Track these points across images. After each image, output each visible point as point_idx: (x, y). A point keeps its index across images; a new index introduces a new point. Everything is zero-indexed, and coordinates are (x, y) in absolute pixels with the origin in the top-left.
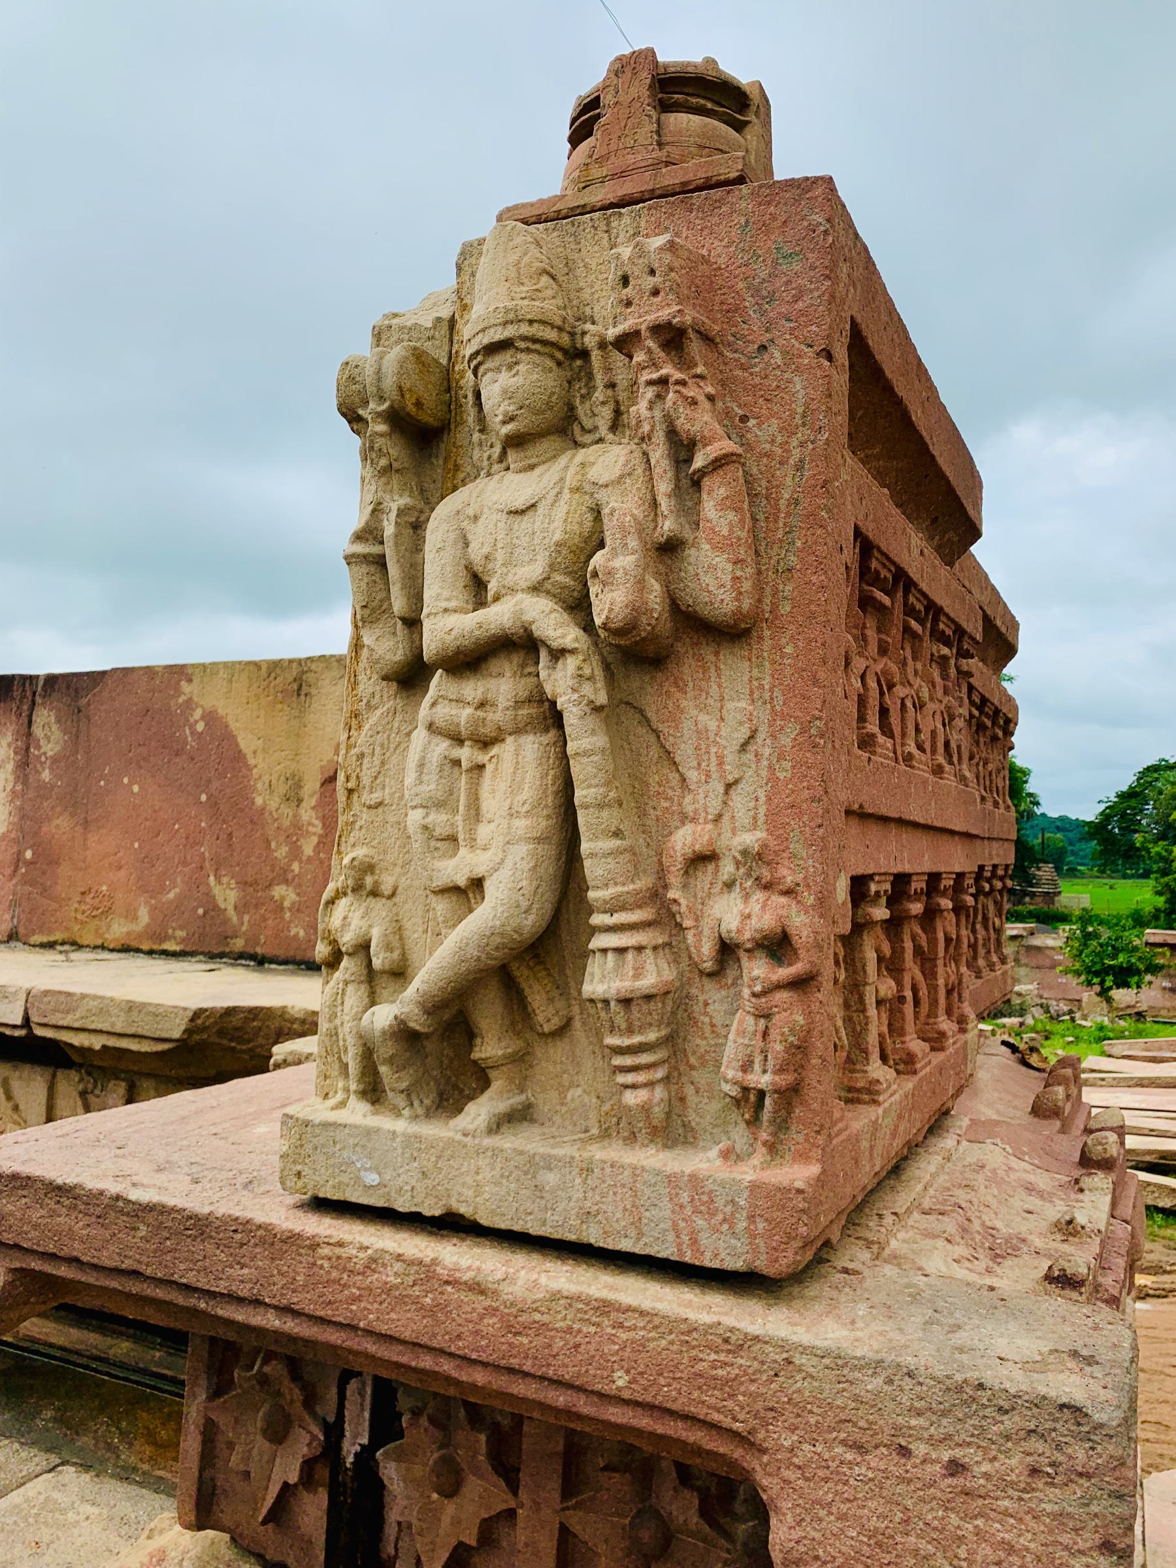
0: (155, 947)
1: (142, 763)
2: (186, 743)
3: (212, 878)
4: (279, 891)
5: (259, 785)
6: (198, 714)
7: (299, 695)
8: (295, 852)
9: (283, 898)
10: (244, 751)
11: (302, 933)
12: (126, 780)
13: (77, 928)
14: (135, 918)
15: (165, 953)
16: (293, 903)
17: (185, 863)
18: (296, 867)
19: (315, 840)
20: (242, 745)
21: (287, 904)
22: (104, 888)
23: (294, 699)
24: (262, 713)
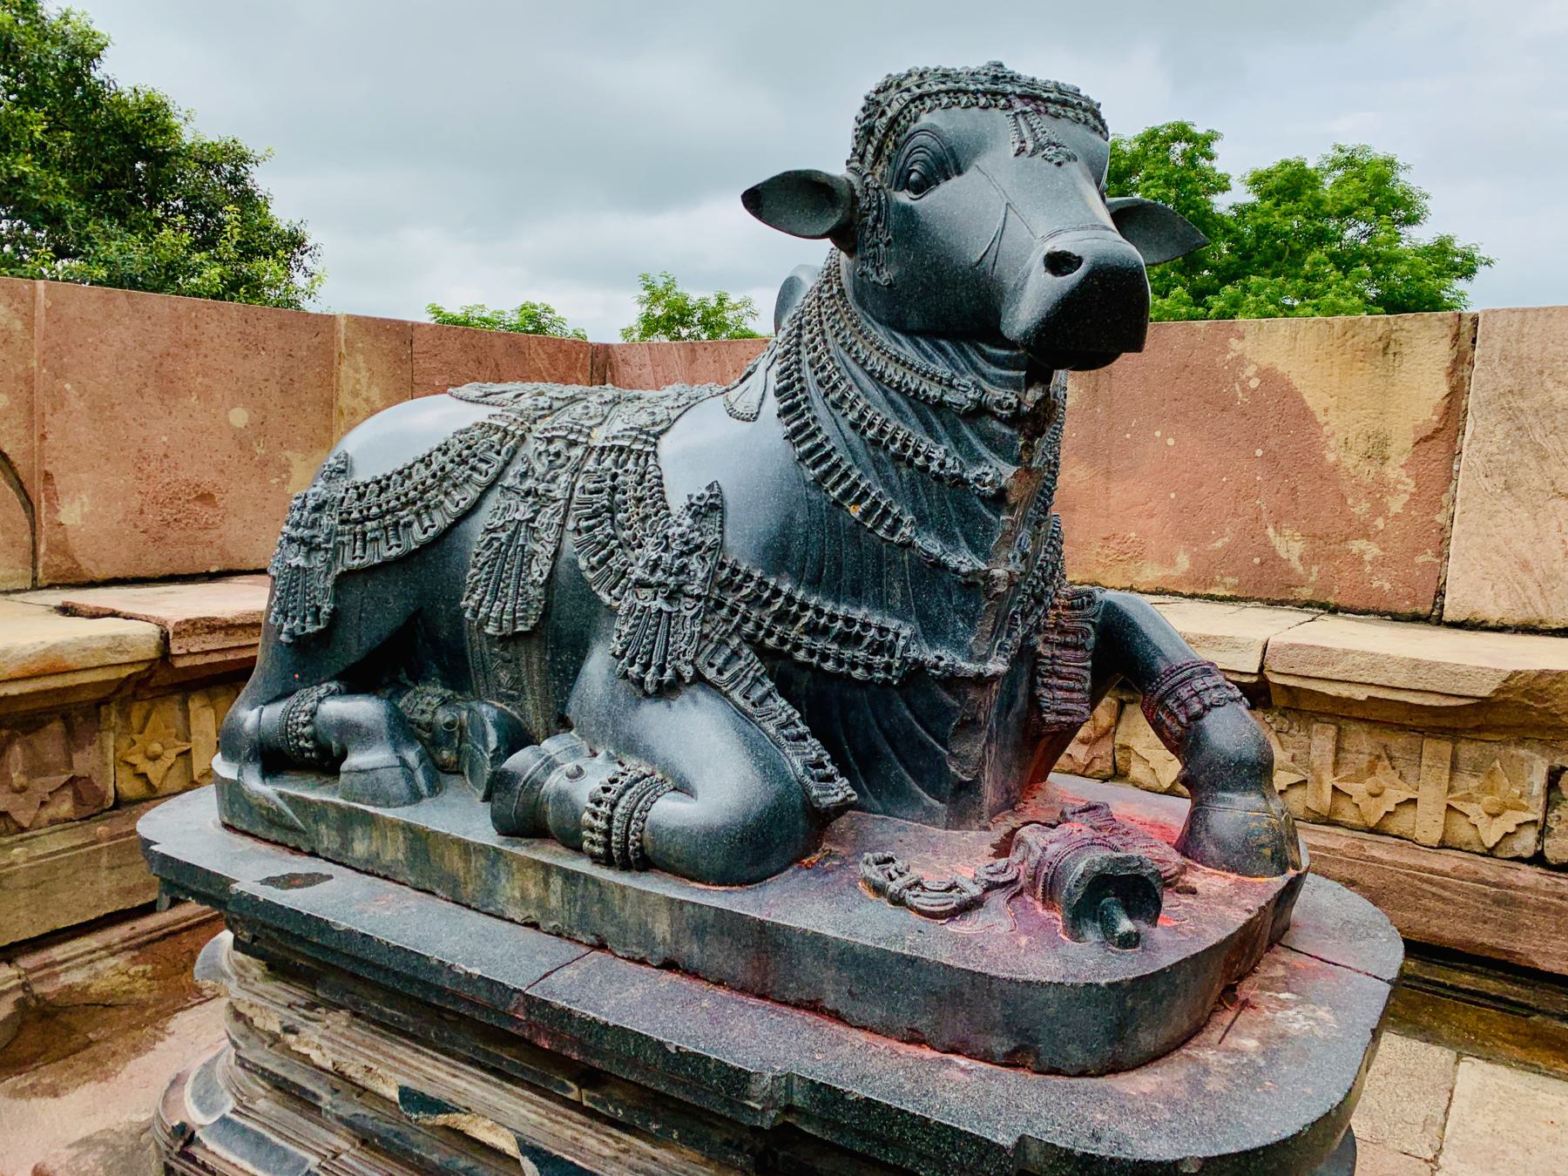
0: (1198, 592)
2: (1235, 398)
3: (1271, 530)
4: (1357, 546)
5: (1332, 443)
6: (1251, 370)
7: (1385, 354)
8: (1379, 509)
9: (1362, 553)
11: (1387, 586)
12: (1158, 434)
13: (1099, 570)
14: (1173, 564)
15: (1212, 598)
16: (1375, 558)
17: (1235, 514)
18: (1380, 523)
19: (1406, 497)
20: (1310, 402)
21: (1367, 558)
23: (1380, 358)
24: (1336, 371)
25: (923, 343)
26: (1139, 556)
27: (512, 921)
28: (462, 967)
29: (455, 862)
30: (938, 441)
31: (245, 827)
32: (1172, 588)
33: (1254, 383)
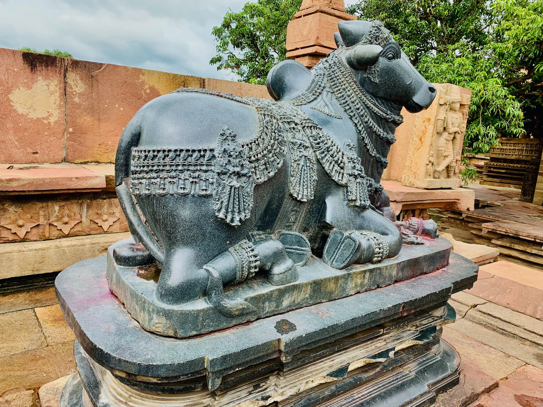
1: (124, 100)
12: (117, 106)
22: (110, 143)
25: (379, 101)
27: (351, 295)
28: (386, 308)
29: (332, 286)
33: (148, 91)
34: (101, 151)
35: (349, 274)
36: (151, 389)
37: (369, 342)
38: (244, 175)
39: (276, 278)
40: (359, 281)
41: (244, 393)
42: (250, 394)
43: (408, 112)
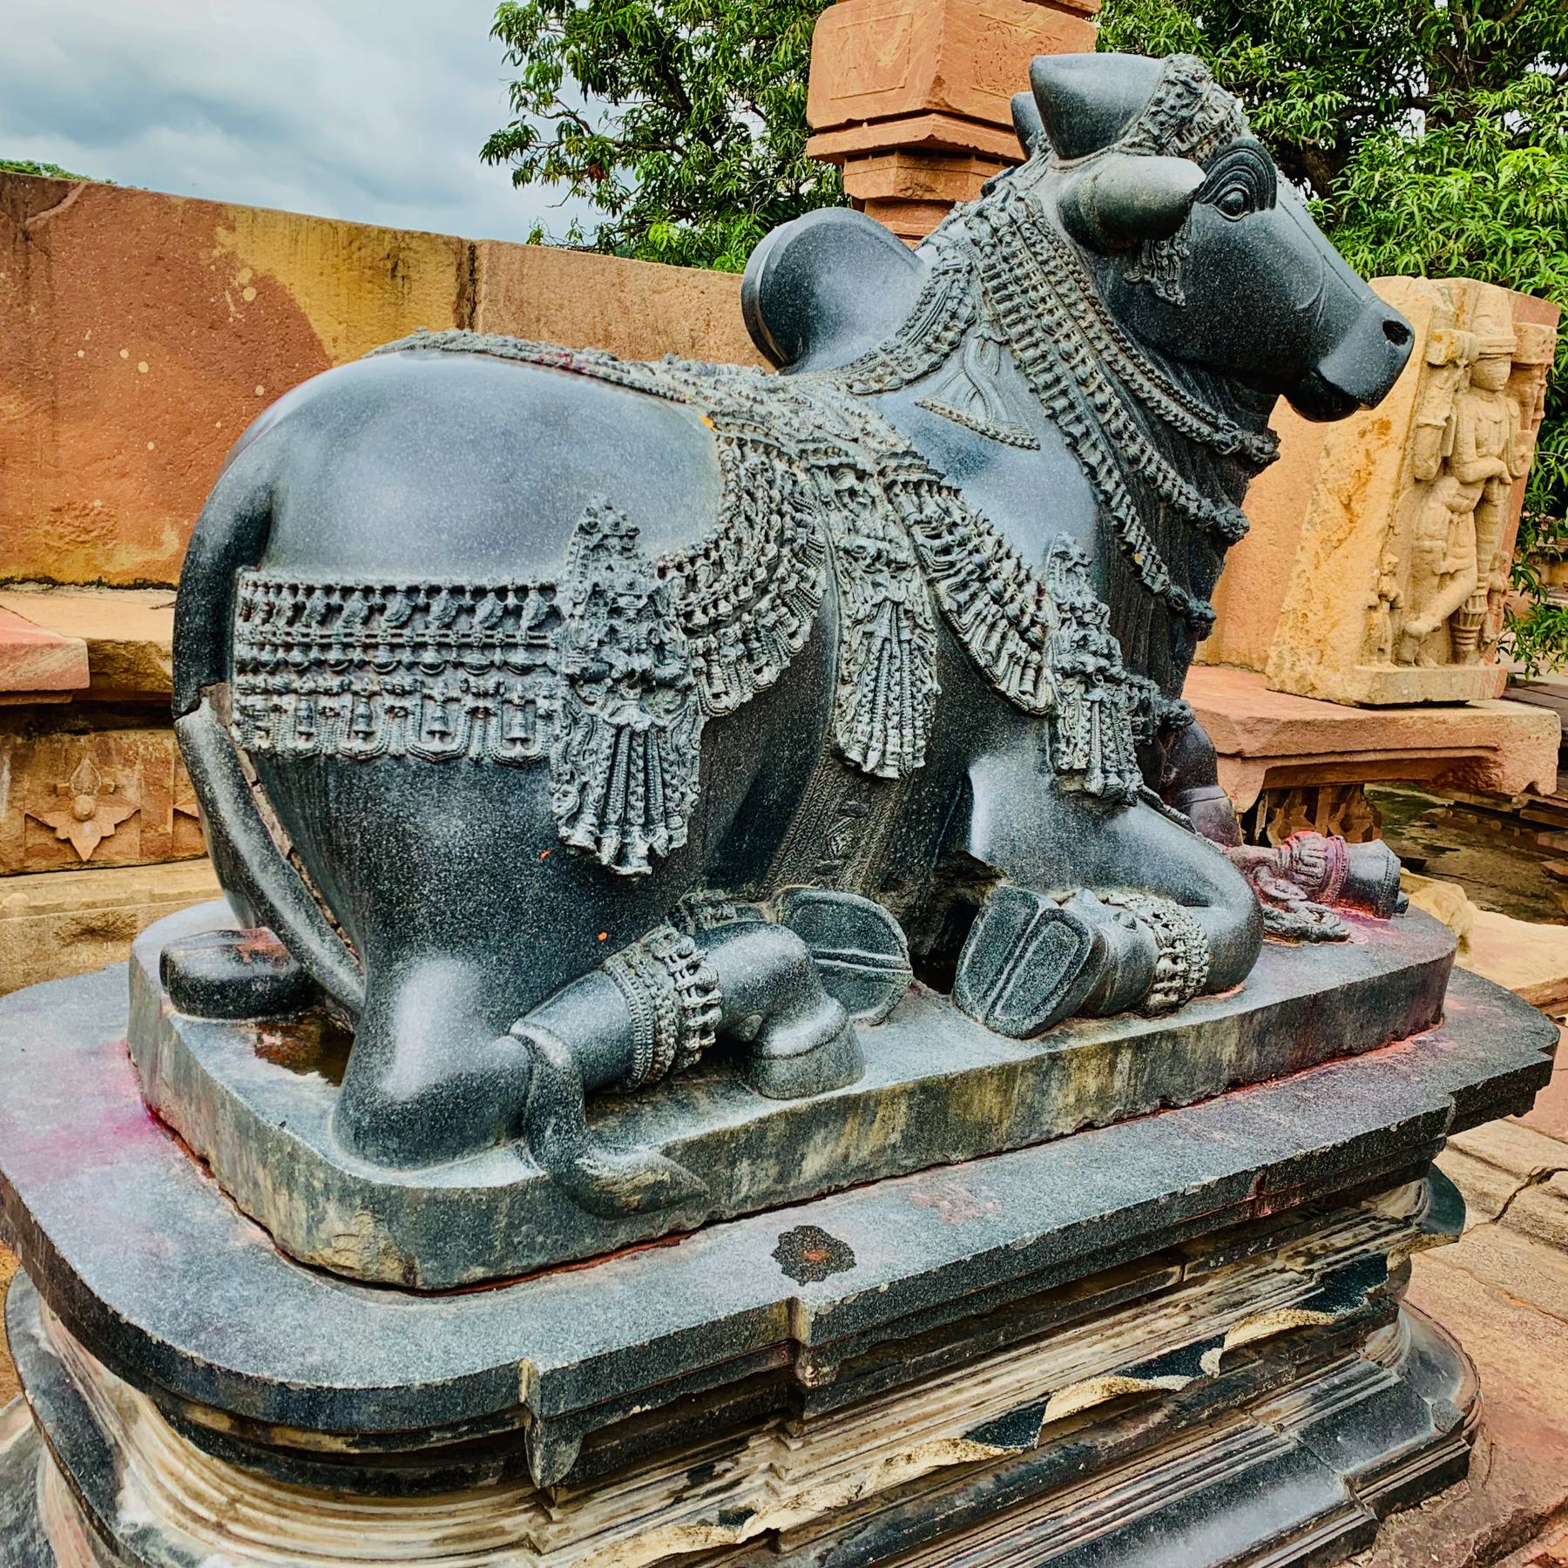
6: (244, 276)
7: (394, 276)
10: (320, 336)
12: (124, 354)
14: (157, 544)
22: (98, 503)
23: (388, 280)
24: (344, 291)
25: (1186, 375)
26: (109, 535)
27: (1062, 1136)
28: (1192, 1186)
29: (988, 1101)
30: (1188, 480)
31: (479, 1272)
32: (155, 578)
33: (249, 295)
34: (61, 537)
35: (1054, 1058)
36: (315, 1478)
37: (1124, 1315)
38: (668, 684)
39: (779, 1071)
40: (1092, 1084)
41: (654, 1498)
42: (678, 1500)
43: (1297, 417)
